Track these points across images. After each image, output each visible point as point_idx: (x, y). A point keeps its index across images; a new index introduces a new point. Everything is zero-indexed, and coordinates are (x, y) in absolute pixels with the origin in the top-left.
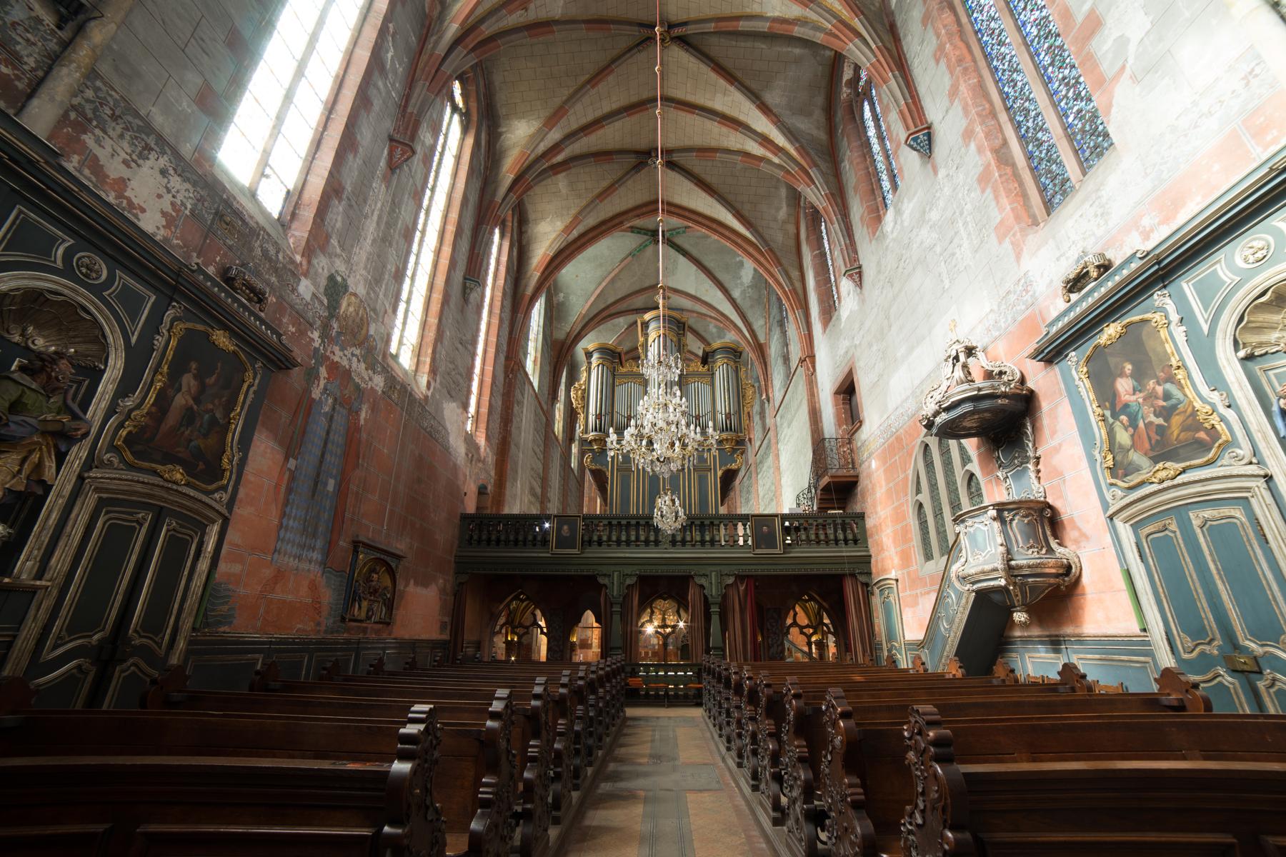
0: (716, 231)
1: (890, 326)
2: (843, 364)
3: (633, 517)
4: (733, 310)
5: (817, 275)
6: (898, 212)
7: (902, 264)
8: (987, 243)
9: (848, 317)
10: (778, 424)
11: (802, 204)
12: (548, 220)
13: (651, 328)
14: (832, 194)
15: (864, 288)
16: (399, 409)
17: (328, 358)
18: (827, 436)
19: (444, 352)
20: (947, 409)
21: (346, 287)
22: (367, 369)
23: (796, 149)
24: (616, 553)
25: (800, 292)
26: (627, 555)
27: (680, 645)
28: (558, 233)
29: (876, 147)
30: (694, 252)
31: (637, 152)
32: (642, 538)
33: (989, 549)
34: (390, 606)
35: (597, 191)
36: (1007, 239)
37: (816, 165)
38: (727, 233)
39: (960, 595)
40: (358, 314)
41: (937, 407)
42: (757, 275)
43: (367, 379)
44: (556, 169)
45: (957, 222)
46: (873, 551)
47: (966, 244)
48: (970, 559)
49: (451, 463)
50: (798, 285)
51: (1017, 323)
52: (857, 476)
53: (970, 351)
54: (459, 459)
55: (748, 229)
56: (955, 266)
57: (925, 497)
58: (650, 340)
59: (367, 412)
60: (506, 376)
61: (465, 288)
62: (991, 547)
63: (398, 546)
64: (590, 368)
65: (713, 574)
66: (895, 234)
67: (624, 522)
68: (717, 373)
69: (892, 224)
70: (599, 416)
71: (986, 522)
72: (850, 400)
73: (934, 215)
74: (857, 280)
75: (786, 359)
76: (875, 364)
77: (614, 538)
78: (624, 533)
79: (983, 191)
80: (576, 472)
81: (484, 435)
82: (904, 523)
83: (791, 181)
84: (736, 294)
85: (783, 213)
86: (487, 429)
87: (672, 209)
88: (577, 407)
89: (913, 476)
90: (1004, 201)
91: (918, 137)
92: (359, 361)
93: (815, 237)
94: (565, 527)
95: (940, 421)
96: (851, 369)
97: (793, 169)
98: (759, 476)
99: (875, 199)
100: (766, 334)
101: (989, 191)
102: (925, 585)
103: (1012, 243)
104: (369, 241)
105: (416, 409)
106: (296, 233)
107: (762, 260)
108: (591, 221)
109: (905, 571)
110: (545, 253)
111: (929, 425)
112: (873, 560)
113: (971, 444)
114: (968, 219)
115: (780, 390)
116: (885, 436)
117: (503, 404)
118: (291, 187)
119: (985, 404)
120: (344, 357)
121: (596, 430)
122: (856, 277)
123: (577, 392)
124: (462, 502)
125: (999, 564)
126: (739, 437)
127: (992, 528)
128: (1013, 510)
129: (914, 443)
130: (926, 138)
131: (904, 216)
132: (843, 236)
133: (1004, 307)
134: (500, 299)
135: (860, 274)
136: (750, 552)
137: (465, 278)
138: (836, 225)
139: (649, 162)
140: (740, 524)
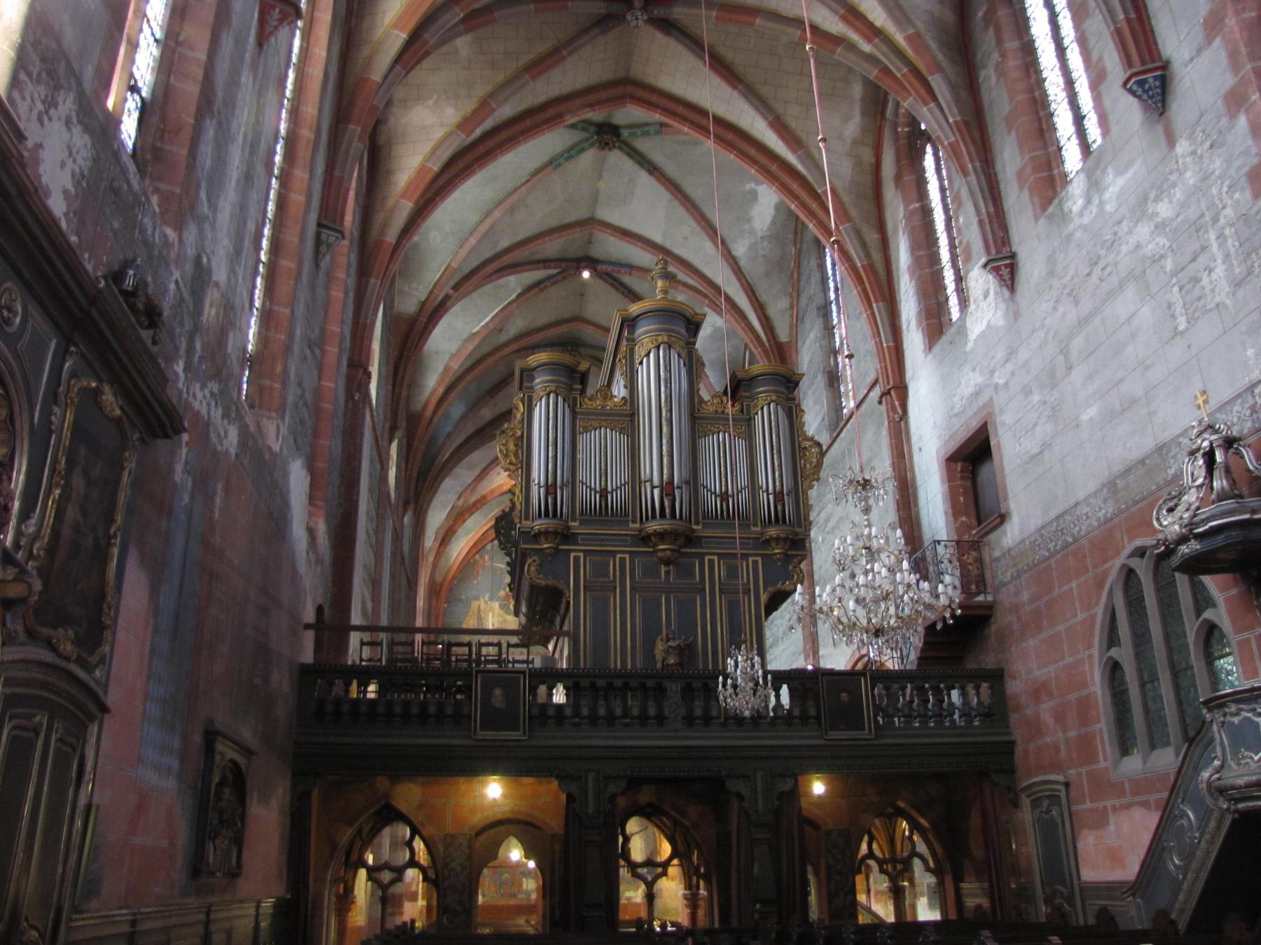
0: (684, 119)
1: (1070, 368)
2: (970, 413)
3: (619, 675)
4: (734, 278)
5: (914, 248)
7: (1097, 271)
9: (983, 335)
11: (889, 112)
12: (430, 102)
13: (640, 331)
14: (966, 123)
21: (209, 272)
22: (223, 418)
28: (447, 129)
30: (670, 169)
32: (635, 712)
35: (526, 59)
38: (752, 152)
40: (218, 321)
43: (222, 434)
45: (1207, 232)
46: (1018, 734)
50: (877, 257)
53: (1229, 443)
55: (794, 151)
56: (1199, 299)
57: (1124, 654)
58: (639, 351)
61: (318, 241)
66: (1086, 220)
67: (601, 683)
69: (1080, 202)
70: (550, 489)
73: (1164, 210)
74: (1007, 277)
76: (1035, 425)
77: (585, 711)
78: (601, 702)
83: (886, 84)
84: (740, 249)
89: (1105, 614)
92: (216, 403)
93: (914, 177)
94: (498, 692)
97: (899, 70)
108: (507, 111)
112: (1019, 749)
114: (1227, 232)
116: (1051, 546)
122: (1005, 272)
126: (796, 534)
129: (1107, 566)
130: (1157, 83)
131: (1107, 196)
132: (984, 199)
135: (1013, 268)
137: (320, 225)
139: (629, 17)
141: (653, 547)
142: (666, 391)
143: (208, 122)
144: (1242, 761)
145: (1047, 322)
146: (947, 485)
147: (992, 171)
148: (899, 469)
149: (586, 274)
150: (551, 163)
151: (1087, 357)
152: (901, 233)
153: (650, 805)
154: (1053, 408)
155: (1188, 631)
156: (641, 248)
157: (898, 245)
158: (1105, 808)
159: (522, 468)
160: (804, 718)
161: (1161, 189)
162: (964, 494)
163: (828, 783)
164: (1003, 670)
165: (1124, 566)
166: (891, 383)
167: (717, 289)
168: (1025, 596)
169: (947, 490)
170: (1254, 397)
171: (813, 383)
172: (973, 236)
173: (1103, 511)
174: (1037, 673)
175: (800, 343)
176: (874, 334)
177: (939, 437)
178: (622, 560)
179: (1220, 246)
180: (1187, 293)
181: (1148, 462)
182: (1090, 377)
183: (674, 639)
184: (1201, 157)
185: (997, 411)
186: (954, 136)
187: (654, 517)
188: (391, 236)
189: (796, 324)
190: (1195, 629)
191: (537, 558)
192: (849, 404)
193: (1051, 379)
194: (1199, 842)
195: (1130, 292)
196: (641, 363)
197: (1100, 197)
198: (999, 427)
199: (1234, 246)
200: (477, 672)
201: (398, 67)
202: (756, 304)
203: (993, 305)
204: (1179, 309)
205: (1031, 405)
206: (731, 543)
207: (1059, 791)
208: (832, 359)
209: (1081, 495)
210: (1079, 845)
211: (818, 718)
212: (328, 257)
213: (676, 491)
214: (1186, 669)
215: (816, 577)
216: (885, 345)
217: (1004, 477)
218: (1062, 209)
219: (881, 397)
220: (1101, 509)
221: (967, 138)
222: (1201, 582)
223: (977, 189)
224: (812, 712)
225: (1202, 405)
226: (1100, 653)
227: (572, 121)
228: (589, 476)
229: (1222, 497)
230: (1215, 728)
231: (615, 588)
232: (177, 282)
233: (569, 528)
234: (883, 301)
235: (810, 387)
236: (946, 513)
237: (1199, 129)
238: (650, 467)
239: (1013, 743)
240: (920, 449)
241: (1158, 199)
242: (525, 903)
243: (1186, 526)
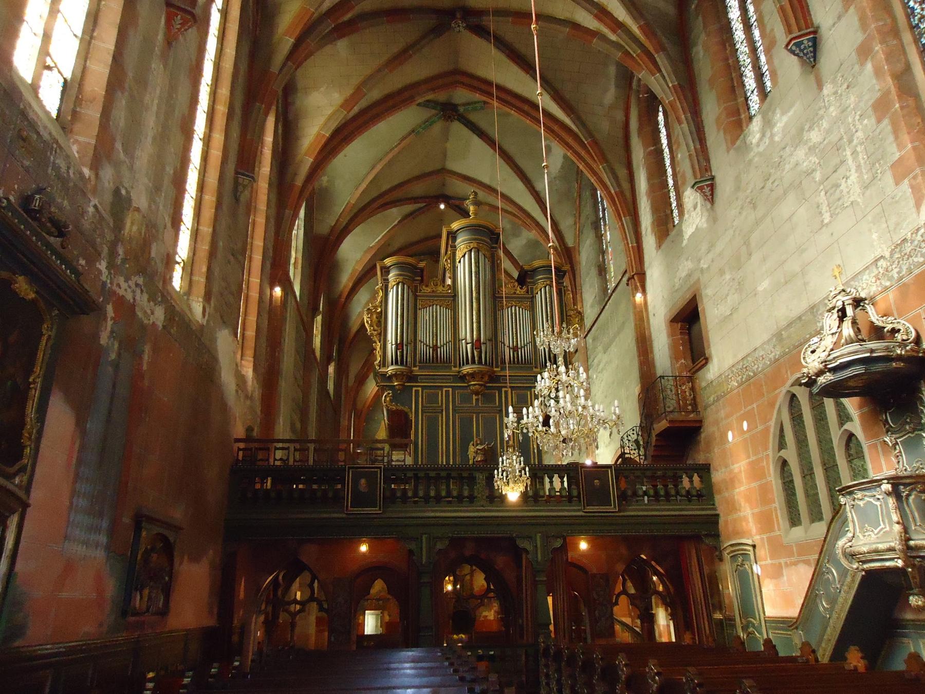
5: (650, 178)
6: (768, 123)
7: (769, 184)
8: (880, 180)
10: (590, 346)
12: (322, 89)
13: (459, 240)
15: (716, 205)
17: (114, 293)
18: (659, 372)
20: (834, 370)
21: (129, 200)
22: (149, 301)
23: (640, 27)
24: (425, 511)
25: (628, 194)
26: (438, 514)
29: (739, 34)
31: (439, 12)
32: (455, 493)
33: (882, 526)
34: (167, 591)
36: (906, 181)
37: (661, 48)
39: (844, 573)
40: (140, 233)
41: (821, 366)
42: (568, 164)
43: (149, 312)
44: (342, 30)
46: (721, 509)
47: (854, 177)
48: (858, 533)
50: (626, 186)
51: (913, 275)
52: (701, 421)
53: (858, 302)
55: (569, 116)
56: (839, 199)
57: (791, 454)
58: (459, 255)
61: (236, 183)
62: (884, 523)
65: (539, 535)
66: (761, 149)
68: (538, 296)
69: (758, 136)
70: (399, 346)
71: (878, 496)
72: (689, 329)
73: (815, 136)
74: (708, 194)
75: (602, 270)
76: (728, 295)
77: (421, 493)
79: (879, 121)
80: (332, 397)
81: (251, 365)
82: (764, 481)
83: (629, 63)
85: (611, 95)
86: (255, 357)
87: (483, 87)
88: (372, 334)
89: (775, 427)
90: (906, 138)
91: (801, 42)
92: (142, 291)
94: (363, 481)
95: (824, 381)
96: (695, 296)
97: (635, 51)
99: (736, 99)
100: (575, 238)
101: (886, 122)
102: (791, 554)
103: (912, 187)
104: (149, 139)
106: (81, 139)
107: (583, 153)
108: (375, 94)
109: (765, 536)
110: (319, 134)
113: (851, 404)
114: (859, 149)
115: (592, 306)
116: (739, 378)
118: (68, 75)
119: (879, 367)
120: (129, 290)
121: (397, 363)
122: (707, 190)
123: (372, 315)
125: (896, 544)
127: (886, 504)
128: (910, 484)
130: (810, 44)
131: (776, 129)
133: (897, 256)
134: (266, 191)
135: (712, 187)
136: (579, 510)
137: (237, 173)
138: (685, 125)
140: (556, 476)
141: (468, 383)
142: (475, 280)
143: (119, 94)
144: (866, 534)
145: (735, 224)
146: (671, 339)
147: (699, 119)
149: (442, 206)
150: (413, 131)
152: (642, 168)
154: (739, 283)
157: (640, 177)
158: (780, 564)
160: (570, 498)
161: (813, 121)
162: (683, 345)
163: (589, 542)
164: (710, 465)
165: (789, 391)
166: (635, 270)
170: (877, 268)
172: (685, 166)
173: (773, 354)
175: (581, 248)
176: (623, 238)
178: (447, 392)
179: (854, 159)
180: (831, 194)
181: (803, 318)
183: (481, 444)
184: (841, 95)
186: (673, 96)
187: (468, 363)
188: (299, 181)
190: (838, 438)
192: (612, 285)
194: (840, 592)
195: (791, 197)
196: (460, 262)
197: (771, 132)
198: (704, 298)
199: (863, 159)
200: (349, 468)
201: (290, 63)
203: (700, 213)
204: (824, 208)
205: (724, 282)
206: (532, 380)
207: (749, 551)
208: (601, 257)
209: (758, 343)
211: (579, 496)
212: (247, 193)
213: (482, 346)
214: (834, 466)
216: (630, 245)
217: (707, 332)
218: (745, 143)
219: (628, 281)
220: (772, 352)
221: (682, 97)
222: (842, 404)
223: (688, 133)
224: (575, 493)
225: (838, 276)
227: (420, 101)
228: (425, 336)
229: (850, 341)
230: (848, 508)
231: (442, 410)
232: (95, 206)
233: (412, 371)
237: (840, 75)
238: (466, 332)
240: (654, 315)
241: (811, 128)
243: (822, 363)
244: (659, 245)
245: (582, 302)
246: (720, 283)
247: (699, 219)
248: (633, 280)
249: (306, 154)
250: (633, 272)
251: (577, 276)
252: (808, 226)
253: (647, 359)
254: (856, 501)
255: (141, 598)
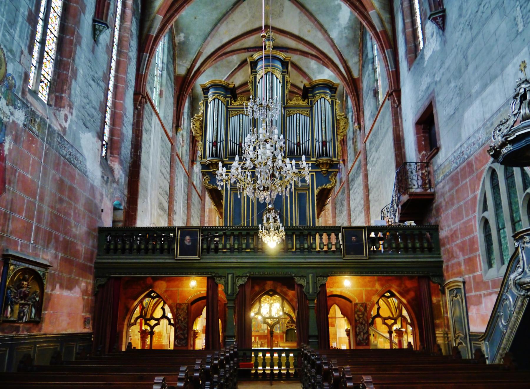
1: (467, 66)
2: (425, 98)
3: (245, 229)
4: (332, 49)
9: (431, 57)
10: (368, 148)
15: (446, 31)
16: (39, 139)
18: (408, 160)
19: (78, 89)
20: (512, 142)
22: (7, 105)
24: (230, 258)
25: (390, 33)
26: (239, 261)
27: (285, 329)
34: (39, 307)
43: (9, 114)
46: (444, 257)
49: (89, 185)
50: (388, 26)
54: (96, 181)
57: (490, 215)
58: (258, 77)
59: (10, 143)
60: (135, 108)
61: (94, 29)
63: (45, 257)
64: (207, 102)
65: (310, 276)
70: (215, 144)
75: (376, 93)
76: (452, 99)
84: (334, 34)
95: (506, 151)
98: (351, 192)
102: (488, 288)
105: (55, 140)
111: (496, 156)
115: (369, 119)
116: (458, 161)
117: (133, 133)
121: (212, 156)
122: (439, 20)
124: (100, 217)
126: (333, 161)
129: (482, 168)
135: (444, 18)
136: (341, 258)
137: (94, 21)
145: (458, 43)
148: (396, 131)
151: (475, 58)
153: (271, 290)
155: (519, 200)
156: (289, 38)
158: (481, 295)
159: (202, 135)
162: (424, 140)
164: (438, 226)
165: (490, 167)
166: (393, 88)
167: (327, 57)
168: (447, 188)
169: (416, 138)
171: (367, 96)
173: (481, 140)
174: (452, 227)
176: (386, 66)
177: (413, 113)
180: (524, 8)
182: (477, 68)
185: (436, 95)
189: (362, 68)
191: (208, 176)
193: (459, 73)
195: (496, 16)
196: (259, 83)
202: (342, 60)
203: (435, 40)
204: (519, 19)
210: (470, 314)
215: (369, 187)
216: (390, 70)
226: (479, 215)
234: (390, 48)
235: (366, 98)
236: (416, 150)
239: (442, 262)
240: (406, 120)
242: (262, 334)
243: (503, 137)
244: (409, 69)
245: (363, 117)
246: (448, 91)
247: (435, 43)
248: (392, 96)
249: (158, 12)
250: (392, 89)
251: (361, 99)
252: (508, 36)
253: (401, 153)
254: (525, 244)
255: (12, 310)
